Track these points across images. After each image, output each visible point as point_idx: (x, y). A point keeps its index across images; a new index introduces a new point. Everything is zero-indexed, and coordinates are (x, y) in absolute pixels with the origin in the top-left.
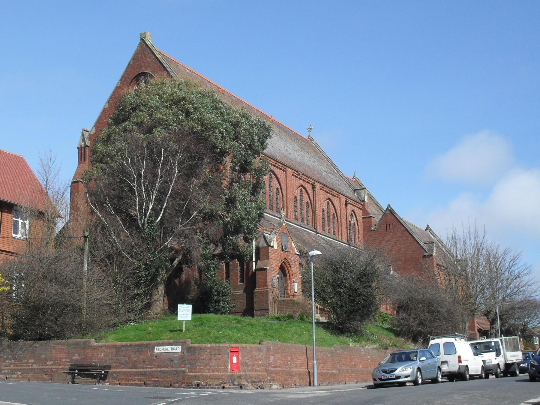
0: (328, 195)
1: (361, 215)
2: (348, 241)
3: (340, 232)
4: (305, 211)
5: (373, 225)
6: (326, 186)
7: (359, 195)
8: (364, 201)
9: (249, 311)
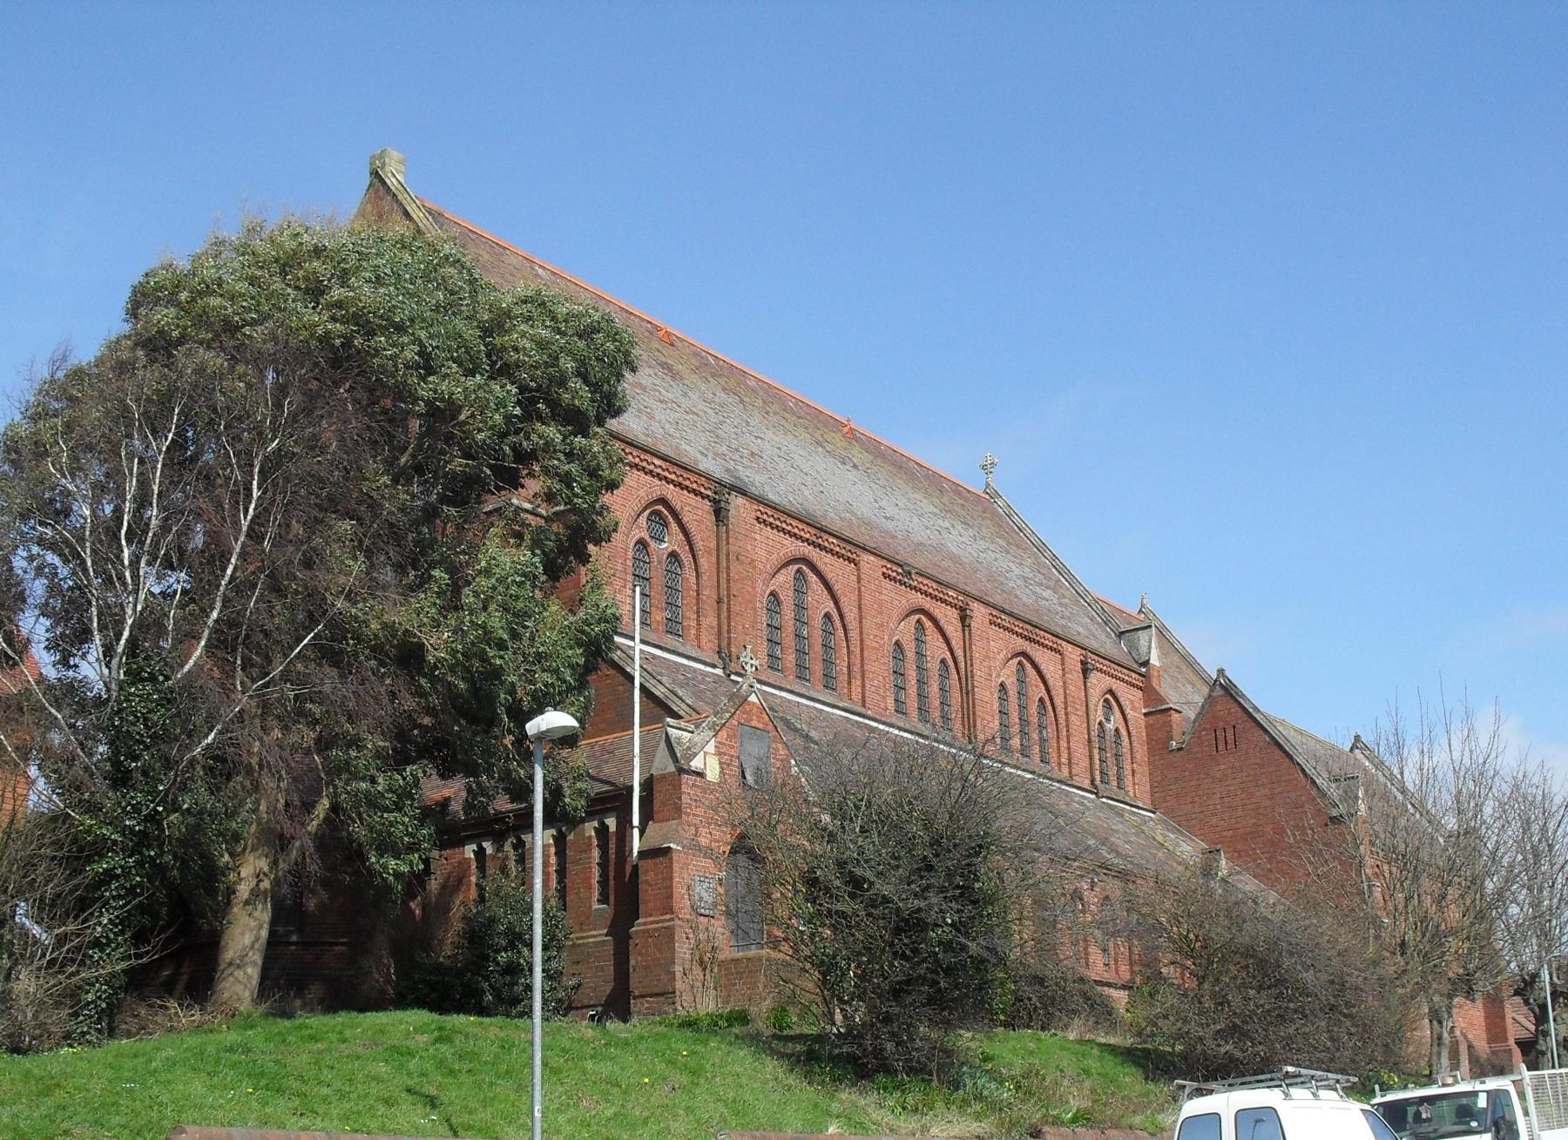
0: (1020, 640)
1: (1139, 703)
2: (1093, 781)
3: (1065, 756)
4: (934, 688)
5: (1176, 732)
6: (1011, 615)
7: (1133, 647)
8: (1146, 663)
9: (618, 1005)
